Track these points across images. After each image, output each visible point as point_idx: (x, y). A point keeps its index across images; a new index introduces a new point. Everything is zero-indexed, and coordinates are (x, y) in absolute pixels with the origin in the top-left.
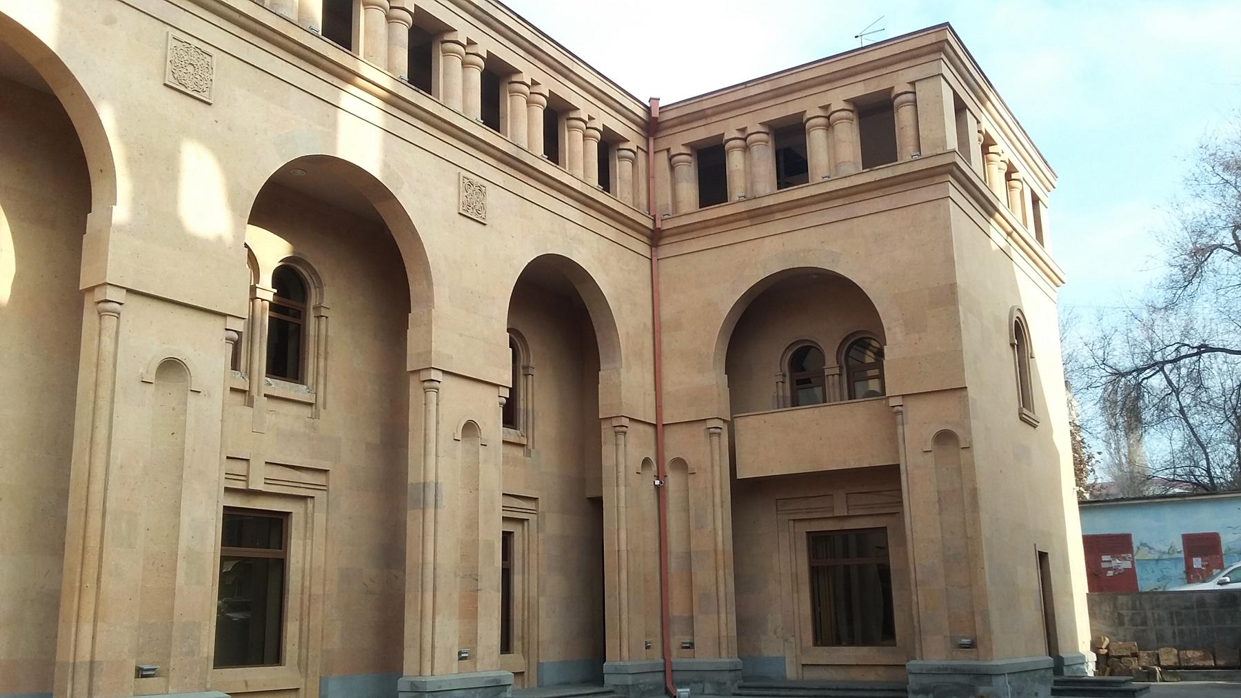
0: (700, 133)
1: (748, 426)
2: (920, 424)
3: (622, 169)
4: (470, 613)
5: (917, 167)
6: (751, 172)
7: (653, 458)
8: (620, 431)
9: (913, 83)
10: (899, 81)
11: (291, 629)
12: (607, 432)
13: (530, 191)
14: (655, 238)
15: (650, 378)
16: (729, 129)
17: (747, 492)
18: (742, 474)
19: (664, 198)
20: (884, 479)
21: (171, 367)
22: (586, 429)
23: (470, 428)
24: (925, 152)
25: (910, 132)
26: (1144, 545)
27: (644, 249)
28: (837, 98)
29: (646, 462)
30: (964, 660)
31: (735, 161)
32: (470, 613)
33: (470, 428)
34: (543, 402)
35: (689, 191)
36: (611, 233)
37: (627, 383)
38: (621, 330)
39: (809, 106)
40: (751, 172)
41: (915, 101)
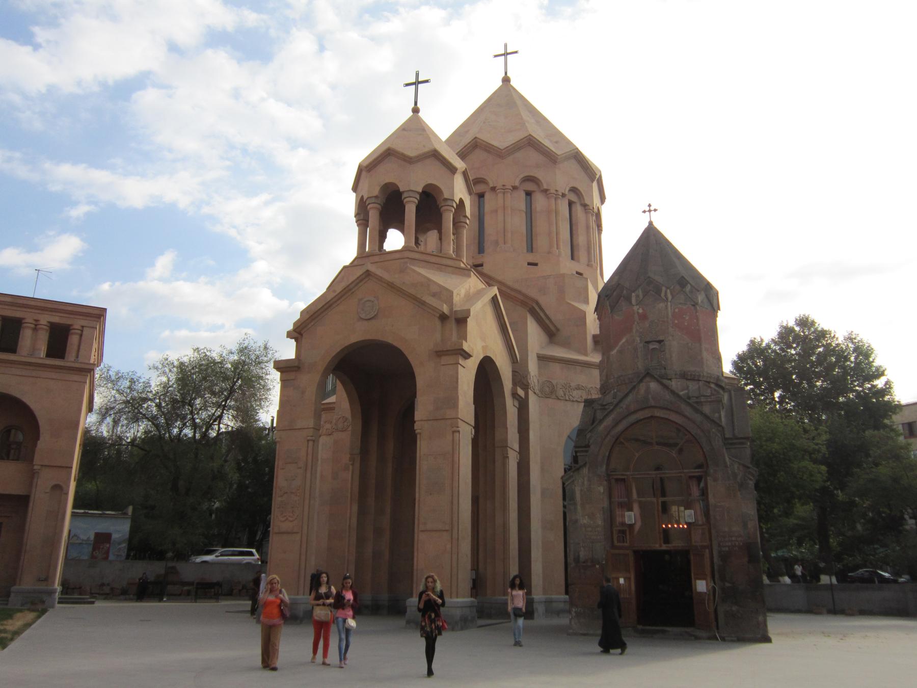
2: (45, 480)
5: (77, 365)
9: (83, 327)
10: (77, 323)
24: (81, 359)
25: (76, 347)
26: (75, 535)
28: (45, 319)
30: (42, 587)
39: (29, 317)
41: (81, 335)
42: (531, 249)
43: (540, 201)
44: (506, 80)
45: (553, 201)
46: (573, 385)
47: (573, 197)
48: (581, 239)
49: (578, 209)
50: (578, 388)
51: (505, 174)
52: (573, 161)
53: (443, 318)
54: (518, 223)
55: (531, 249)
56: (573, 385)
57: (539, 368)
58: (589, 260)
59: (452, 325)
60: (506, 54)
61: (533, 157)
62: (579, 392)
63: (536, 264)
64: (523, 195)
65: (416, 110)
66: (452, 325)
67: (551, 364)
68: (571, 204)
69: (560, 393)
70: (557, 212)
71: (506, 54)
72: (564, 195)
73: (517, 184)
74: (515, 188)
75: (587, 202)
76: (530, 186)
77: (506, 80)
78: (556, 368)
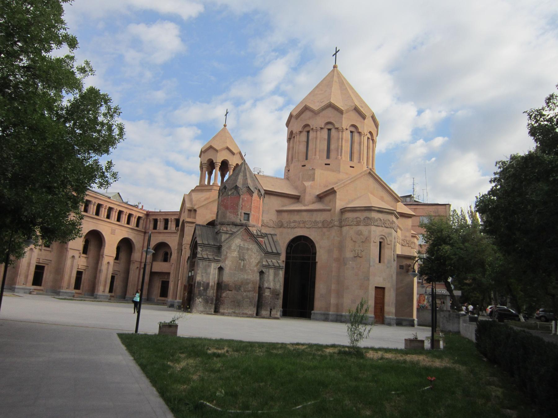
0: (155, 217)
1: (154, 263)
3: (141, 221)
4: (105, 286)
6: (160, 225)
7: (139, 266)
8: (134, 263)
11: (82, 286)
12: (132, 262)
13: (123, 229)
14: (145, 233)
15: (140, 254)
16: (158, 218)
17: (152, 274)
18: (153, 271)
19: (148, 227)
20: (169, 274)
21: (73, 257)
22: (129, 262)
23: (108, 263)
27: (143, 234)
28: (173, 217)
29: (138, 268)
31: (159, 223)
32: (105, 286)
33: (108, 263)
34: (123, 255)
35: (152, 226)
36: (137, 233)
37: (137, 256)
38: (136, 247)
40: (160, 225)
42: (307, 159)
43: (312, 134)
44: (335, 67)
45: (315, 133)
46: (292, 221)
47: (329, 127)
48: (333, 147)
49: (333, 132)
50: (295, 222)
51: (297, 127)
52: (330, 109)
53: (190, 211)
54: (302, 148)
55: (307, 159)
56: (292, 221)
57: (278, 215)
58: (338, 155)
59: (192, 212)
60: (335, 54)
61: (307, 114)
62: (294, 224)
63: (305, 166)
64: (306, 134)
65: (225, 126)
66: (192, 212)
68: (329, 130)
71: (335, 54)
72: (321, 128)
73: (300, 130)
74: (301, 132)
76: (307, 129)
77: (335, 67)
78: (285, 215)
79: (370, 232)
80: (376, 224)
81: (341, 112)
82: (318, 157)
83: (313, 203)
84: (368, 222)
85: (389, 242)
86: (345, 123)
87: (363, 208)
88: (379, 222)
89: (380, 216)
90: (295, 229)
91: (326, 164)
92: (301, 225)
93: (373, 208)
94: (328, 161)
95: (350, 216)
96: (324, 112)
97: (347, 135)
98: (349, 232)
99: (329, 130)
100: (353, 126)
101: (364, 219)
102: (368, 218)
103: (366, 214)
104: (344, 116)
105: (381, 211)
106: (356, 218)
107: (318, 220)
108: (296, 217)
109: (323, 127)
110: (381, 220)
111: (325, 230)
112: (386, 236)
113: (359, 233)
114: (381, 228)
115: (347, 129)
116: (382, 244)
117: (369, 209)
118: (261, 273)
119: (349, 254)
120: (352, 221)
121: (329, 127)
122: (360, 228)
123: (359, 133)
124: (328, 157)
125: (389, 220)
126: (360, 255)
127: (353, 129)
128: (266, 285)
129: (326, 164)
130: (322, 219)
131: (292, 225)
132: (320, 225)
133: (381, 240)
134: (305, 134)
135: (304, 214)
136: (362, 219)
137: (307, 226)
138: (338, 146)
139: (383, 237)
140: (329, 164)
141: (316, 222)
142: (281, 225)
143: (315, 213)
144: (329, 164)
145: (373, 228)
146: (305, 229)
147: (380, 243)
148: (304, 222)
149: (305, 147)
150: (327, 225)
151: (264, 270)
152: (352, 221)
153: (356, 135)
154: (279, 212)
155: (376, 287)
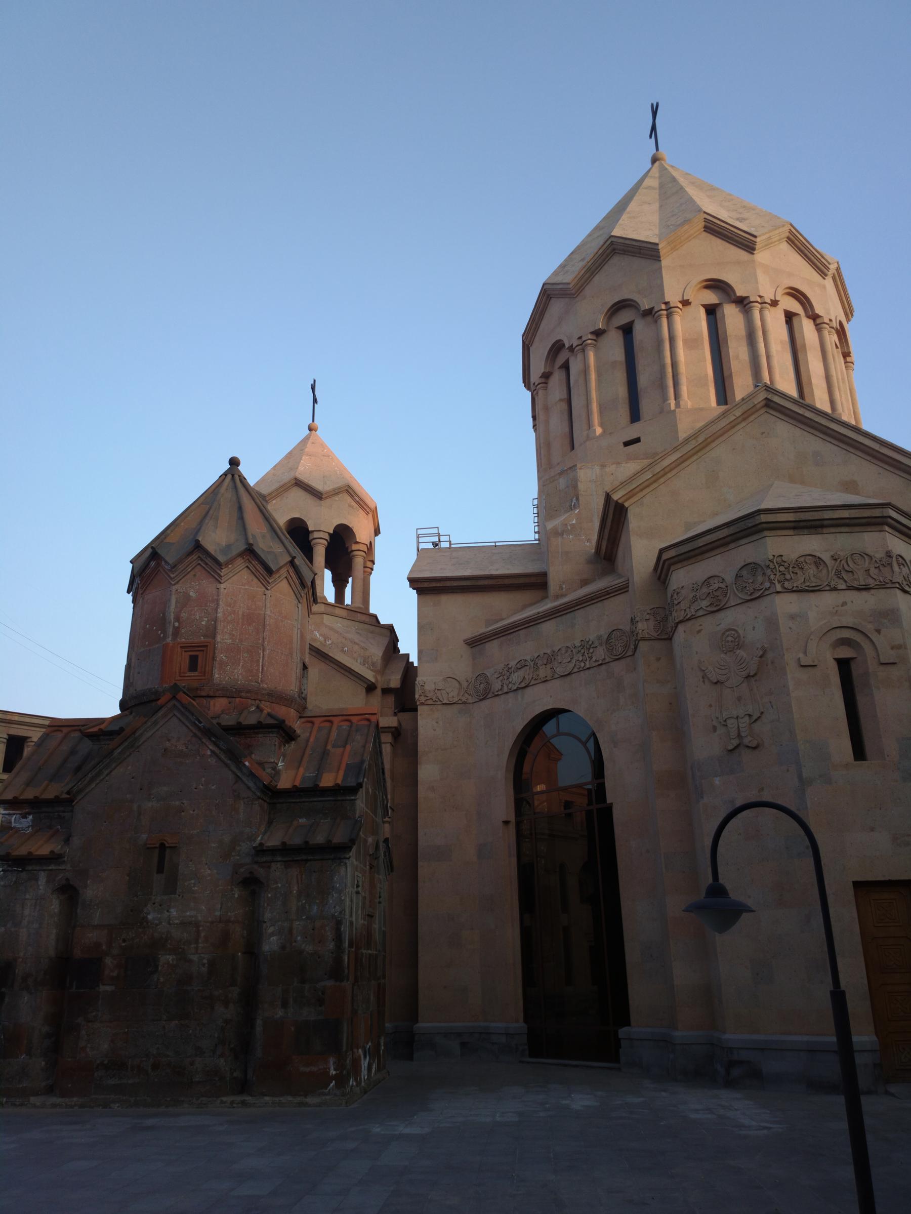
44: (654, 160)
47: (623, 318)
48: (644, 379)
49: (641, 330)
50: (522, 665)
52: (616, 260)
56: (513, 664)
58: (665, 398)
62: (521, 673)
64: (563, 374)
65: (310, 429)
67: (488, 645)
68: (627, 330)
69: (497, 686)
70: (585, 371)
72: (598, 333)
75: (645, 305)
78: (493, 648)
79: (772, 623)
80: (798, 583)
81: (647, 252)
82: (599, 431)
83: (585, 583)
84: (756, 583)
85: (888, 655)
86: (679, 280)
87: (725, 532)
88: (811, 570)
89: (812, 544)
90: (529, 691)
91: (627, 444)
92: (543, 672)
93: (764, 518)
94: (632, 432)
95: (681, 578)
96: (597, 278)
97: (690, 325)
98: (695, 644)
99: (627, 330)
100: (716, 285)
101: (738, 576)
102: (753, 567)
103: (746, 552)
104: (665, 262)
105: (808, 522)
106: (707, 582)
107: (592, 637)
108: (525, 648)
109: (600, 325)
110: (818, 562)
111: (618, 668)
112: (869, 628)
113: (731, 642)
114: (828, 600)
115: (686, 303)
116: (856, 671)
117: (749, 527)
118: (251, 884)
119: (705, 746)
120: (695, 600)
121: (623, 318)
122: (728, 618)
123: (743, 303)
124: (635, 416)
125: (863, 555)
126: (746, 741)
127: (711, 298)
128: (271, 944)
129: (627, 444)
130: (604, 632)
131: (516, 677)
132: (600, 653)
133: (845, 653)
134: (557, 377)
135: (548, 627)
136: (729, 578)
137: (560, 670)
138: (663, 367)
139: (846, 634)
140: (637, 440)
141: (587, 647)
142: (483, 690)
143: (579, 616)
144: (637, 440)
145: (785, 605)
146: (556, 683)
147: (844, 665)
148: (550, 659)
149: (566, 417)
150: (622, 646)
151: (260, 872)
152: (695, 600)
153: (731, 315)
154: (476, 643)
155: (857, 885)
